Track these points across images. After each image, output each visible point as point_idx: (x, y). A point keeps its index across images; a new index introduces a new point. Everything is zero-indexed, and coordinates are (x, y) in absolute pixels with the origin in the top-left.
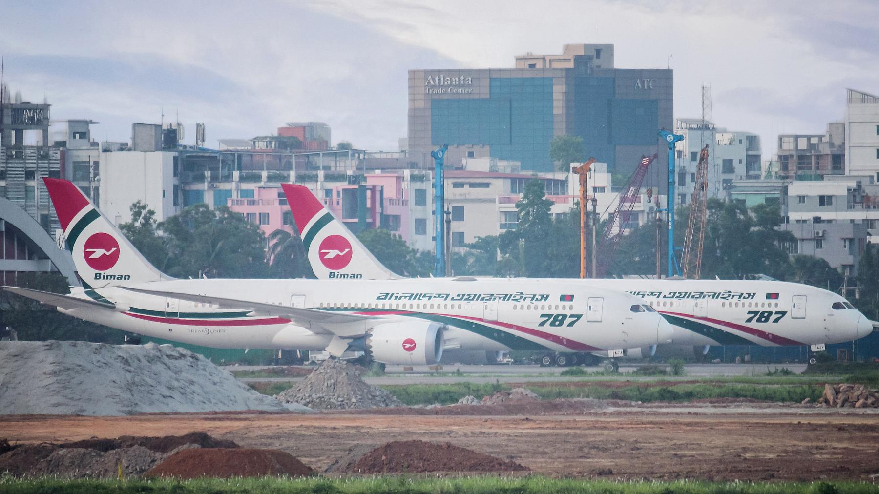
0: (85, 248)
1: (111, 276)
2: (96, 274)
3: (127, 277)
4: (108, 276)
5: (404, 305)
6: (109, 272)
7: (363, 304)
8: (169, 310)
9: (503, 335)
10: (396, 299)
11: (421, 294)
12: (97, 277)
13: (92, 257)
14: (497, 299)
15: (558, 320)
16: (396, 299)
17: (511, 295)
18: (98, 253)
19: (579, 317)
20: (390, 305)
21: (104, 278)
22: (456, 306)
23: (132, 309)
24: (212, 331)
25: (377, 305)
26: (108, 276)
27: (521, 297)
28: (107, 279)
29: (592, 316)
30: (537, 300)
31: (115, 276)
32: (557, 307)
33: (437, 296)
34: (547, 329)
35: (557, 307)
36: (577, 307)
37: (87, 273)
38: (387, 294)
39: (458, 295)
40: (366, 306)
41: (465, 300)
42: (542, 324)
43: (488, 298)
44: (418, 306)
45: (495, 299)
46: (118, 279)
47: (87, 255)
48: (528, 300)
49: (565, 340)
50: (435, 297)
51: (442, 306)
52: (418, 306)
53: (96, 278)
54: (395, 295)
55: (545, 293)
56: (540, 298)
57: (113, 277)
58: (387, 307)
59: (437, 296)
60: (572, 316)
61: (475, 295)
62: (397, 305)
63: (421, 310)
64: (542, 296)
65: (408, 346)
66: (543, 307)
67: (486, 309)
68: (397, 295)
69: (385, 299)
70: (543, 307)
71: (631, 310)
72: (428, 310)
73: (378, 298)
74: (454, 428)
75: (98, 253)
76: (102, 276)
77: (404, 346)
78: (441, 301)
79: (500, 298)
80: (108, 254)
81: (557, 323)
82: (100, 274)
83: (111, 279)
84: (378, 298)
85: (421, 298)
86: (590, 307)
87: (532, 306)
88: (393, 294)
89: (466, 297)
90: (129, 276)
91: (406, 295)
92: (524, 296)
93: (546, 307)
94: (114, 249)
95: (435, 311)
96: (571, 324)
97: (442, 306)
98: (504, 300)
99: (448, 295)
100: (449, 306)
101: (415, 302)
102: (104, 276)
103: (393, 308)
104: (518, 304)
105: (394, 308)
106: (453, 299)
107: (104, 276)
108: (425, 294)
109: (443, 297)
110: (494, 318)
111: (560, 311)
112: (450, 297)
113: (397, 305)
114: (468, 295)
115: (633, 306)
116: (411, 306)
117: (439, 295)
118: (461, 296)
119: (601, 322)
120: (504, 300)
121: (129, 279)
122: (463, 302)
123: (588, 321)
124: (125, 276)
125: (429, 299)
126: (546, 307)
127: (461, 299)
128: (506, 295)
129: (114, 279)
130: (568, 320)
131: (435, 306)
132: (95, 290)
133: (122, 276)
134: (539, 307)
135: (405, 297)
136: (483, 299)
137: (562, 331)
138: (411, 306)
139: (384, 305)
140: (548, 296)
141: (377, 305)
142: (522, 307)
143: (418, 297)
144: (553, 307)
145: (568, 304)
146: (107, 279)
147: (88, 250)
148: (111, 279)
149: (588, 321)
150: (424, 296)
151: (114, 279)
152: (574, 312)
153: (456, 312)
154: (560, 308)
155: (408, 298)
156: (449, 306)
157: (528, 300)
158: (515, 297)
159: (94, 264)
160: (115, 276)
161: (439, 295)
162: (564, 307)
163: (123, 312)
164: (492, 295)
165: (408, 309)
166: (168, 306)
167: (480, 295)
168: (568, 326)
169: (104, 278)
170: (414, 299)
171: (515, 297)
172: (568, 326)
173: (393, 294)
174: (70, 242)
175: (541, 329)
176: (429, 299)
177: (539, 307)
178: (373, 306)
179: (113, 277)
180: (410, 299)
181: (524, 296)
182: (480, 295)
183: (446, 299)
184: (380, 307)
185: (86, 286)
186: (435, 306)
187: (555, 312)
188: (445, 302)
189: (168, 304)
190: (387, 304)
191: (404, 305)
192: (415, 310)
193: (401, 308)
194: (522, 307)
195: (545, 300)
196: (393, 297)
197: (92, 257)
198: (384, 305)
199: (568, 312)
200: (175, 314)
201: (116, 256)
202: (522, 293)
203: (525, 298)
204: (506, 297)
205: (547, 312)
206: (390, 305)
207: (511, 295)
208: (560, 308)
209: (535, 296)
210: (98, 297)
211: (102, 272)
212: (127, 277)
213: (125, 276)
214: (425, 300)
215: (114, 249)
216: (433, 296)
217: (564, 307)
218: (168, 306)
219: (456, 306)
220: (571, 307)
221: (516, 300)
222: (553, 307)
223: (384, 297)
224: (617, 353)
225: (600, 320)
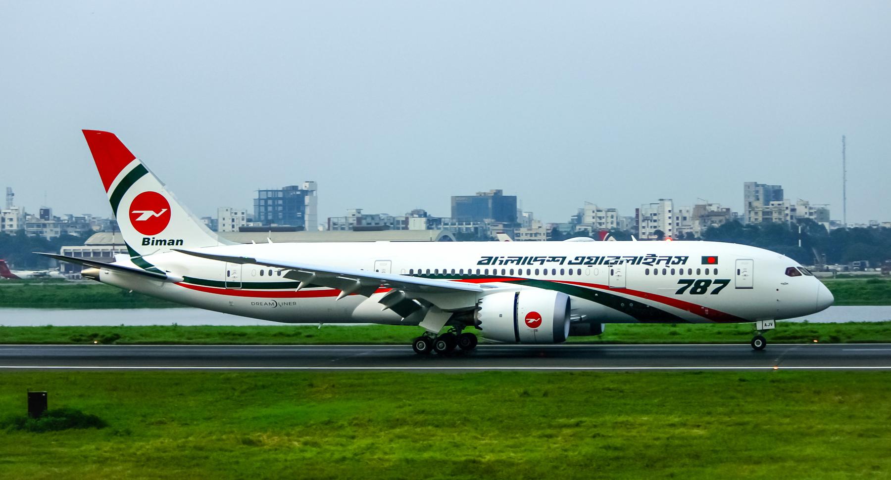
0: (132, 209)
1: (161, 241)
2: (144, 239)
3: (180, 242)
4: (157, 241)
5: (512, 272)
6: (158, 237)
7: (462, 271)
8: (230, 279)
9: (631, 305)
10: (501, 264)
11: (532, 258)
12: (145, 242)
13: (139, 219)
14: (625, 262)
15: (700, 287)
16: (501, 264)
17: (641, 258)
18: (146, 215)
19: (725, 282)
20: (495, 271)
21: (153, 244)
22: (575, 272)
23: (186, 279)
24: (281, 304)
25: (478, 271)
26: (157, 241)
27: (654, 260)
28: (157, 244)
29: (740, 281)
30: (673, 263)
31: (165, 241)
32: (699, 272)
33: (551, 259)
34: (687, 297)
35: (699, 272)
36: (724, 270)
37: (134, 238)
38: (490, 258)
39: (577, 259)
40: (466, 272)
41: (585, 264)
42: (680, 292)
43: (613, 261)
44: (529, 272)
45: (622, 262)
46: (169, 244)
47: (133, 217)
48: (663, 263)
49: (707, 311)
51: (558, 272)
52: (529, 272)
53: (143, 244)
54: (499, 259)
55: (682, 254)
56: (676, 260)
57: (163, 242)
58: (491, 273)
59: (551, 259)
60: (717, 282)
61: (597, 258)
62: (503, 271)
63: (533, 276)
64: (679, 258)
65: (532, 321)
66: (681, 272)
67: (612, 274)
68: (502, 259)
69: (488, 263)
70: (681, 272)
71: (786, 273)
72: (541, 277)
73: (480, 263)
74: (584, 419)
75: (146, 215)
76: (151, 241)
77: (527, 321)
78: (556, 265)
79: (628, 261)
80: (157, 216)
81: (699, 290)
82: (149, 239)
83: (161, 244)
84: (480, 263)
85: (532, 262)
86: (739, 271)
87: (669, 270)
88: (497, 258)
90: (182, 241)
91: (513, 259)
92: (657, 259)
93: (686, 272)
94: (164, 210)
95: (549, 277)
96: (716, 292)
97: (558, 272)
98: (633, 263)
99: (564, 258)
100: (567, 272)
101: (525, 268)
102: (153, 241)
103: (497, 275)
104: (651, 269)
105: (499, 274)
106: (570, 263)
107: (153, 241)
108: (536, 258)
109: (558, 261)
110: (621, 285)
111: (703, 276)
112: (566, 261)
113: (503, 271)
114: (589, 258)
115: (788, 269)
116: (520, 272)
117: (554, 259)
118: (580, 259)
119: (752, 288)
120: (633, 263)
121: (181, 244)
122: (583, 267)
123: (736, 288)
124: (178, 241)
125: (542, 264)
126: (686, 272)
127: (580, 263)
128: (636, 258)
129: (165, 244)
130: (712, 287)
131: (550, 272)
132: (143, 258)
133: (173, 241)
134: (677, 272)
135: (512, 262)
136: (607, 263)
137: (705, 300)
138: (520, 272)
139: (487, 271)
140: (686, 258)
141: (478, 271)
142: (656, 272)
143: (529, 261)
144: (694, 272)
145: (711, 267)
146: (157, 244)
147: (134, 212)
148: (161, 244)
149: (736, 288)
150: (536, 260)
151: (165, 244)
152: (718, 277)
153: (575, 278)
154: (703, 272)
155: (516, 262)
156: (567, 272)
157: (663, 263)
158: (646, 259)
159: (140, 227)
161: (554, 259)
162: (707, 272)
163: (177, 283)
164: (618, 258)
165: (516, 275)
166: (229, 275)
167: (603, 258)
168: (712, 293)
169: (153, 244)
170: (523, 263)
171: (646, 259)
172: (712, 293)
173: (497, 258)
174: (115, 201)
175: (679, 297)
176: (542, 264)
177: (677, 272)
178: (474, 272)
179: (163, 242)
180: (518, 264)
181: (657, 259)
182: (603, 258)
183: (562, 263)
184: (482, 273)
185: (131, 252)
186: (550, 272)
187: (695, 277)
188: (562, 267)
189: (229, 272)
190: (491, 268)
191: (512, 272)
192: (524, 276)
193: (508, 274)
194: (656, 272)
195: (684, 263)
196: (498, 262)
197: (139, 219)
198: (487, 271)
199: (712, 277)
200: (237, 284)
201: (166, 218)
202: (654, 255)
203: (659, 261)
204: (635, 260)
205: (686, 276)
206: (495, 271)
208: (703, 272)
209: (670, 258)
210: (146, 265)
211: (151, 237)
212: (180, 242)
213: (178, 241)
214: (537, 265)
215: (164, 210)
216: (547, 259)
217: (707, 272)
218: (229, 275)
219: (575, 272)
220: (716, 272)
221: (648, 264)
222: (694, 272)
223: (486, 261)
224: (768, 324)
225: (751, 286)
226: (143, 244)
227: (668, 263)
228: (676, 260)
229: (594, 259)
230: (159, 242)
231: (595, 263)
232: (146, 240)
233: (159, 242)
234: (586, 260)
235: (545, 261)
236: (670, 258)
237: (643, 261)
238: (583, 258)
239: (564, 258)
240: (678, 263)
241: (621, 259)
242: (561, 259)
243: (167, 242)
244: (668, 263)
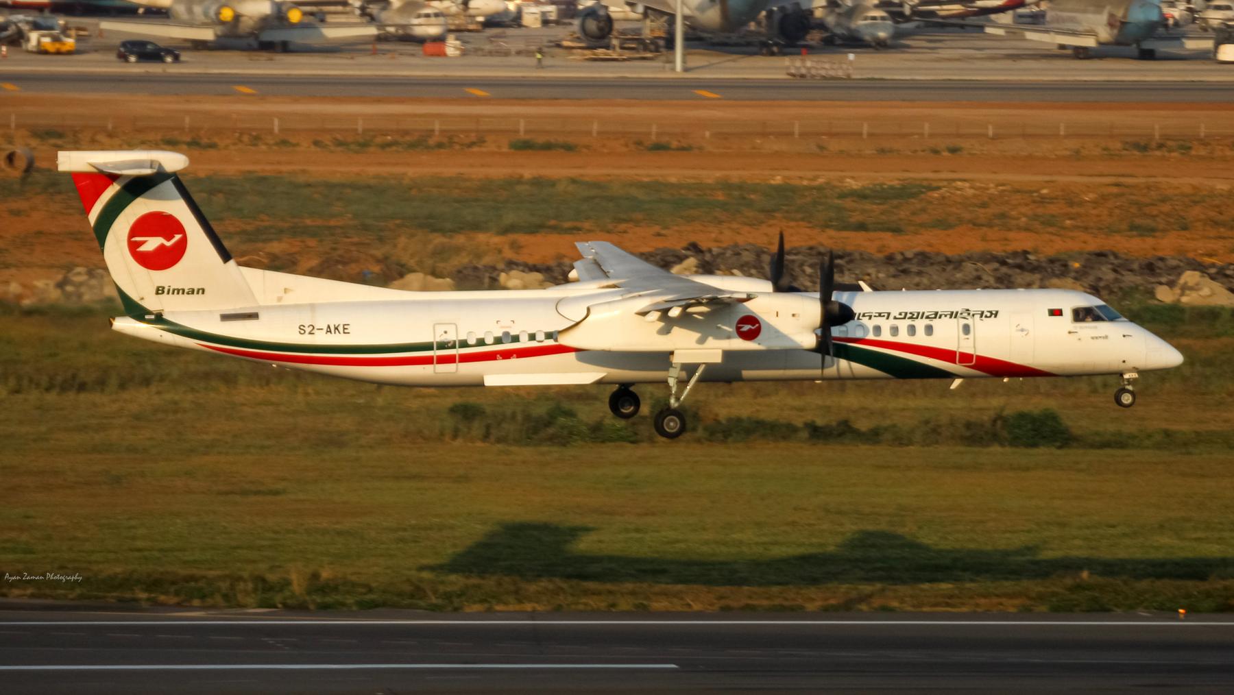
1: (178, 290)
14: (943, 316)
17: (957, 313)
21: (168, 293)
28: (173, 293)
30: (986, 317)
39: (900, 314)
41: (909, 318)
46: (188, 293)
50: (875, 316)
55: (993, 309)
56: (989, 314)
57: (181, 292)
64: (991, 312)
76: (166, 291)
79: (946, 316)
83: (178, 293)
85: (861, 318)
89: (909, 315)
106: (895, 318)
109: (884, 316)
114: (911, 313)
117: (880, 315)
118: (903, 314)
125: (870, 319)
127: (904, 318)
129: (183, 293)
136: (927, 317)
140: (997, 312)
148: (178, 293)
150: (864, 316)
160: (183, 290)
161: (880, 315)
167: (923, 313)
179: (181, 292)
182: (923, 313)
183: (888, 318)
202: (968, 310)
203: (973, 315)
207: (957, 313)
209: (983, 312)
226: (157, 293)
227: (981, 317)
228: (989, 314)
229: (916, 314)
230: (176, 291)
231: (917, 318)
232: (160, 289)
233: (176, 291)
234: (909, 315)
235: (873, 317)
236: (983, 312)
237: (959, 314)
238: (906, 314)
239: (889, 314)
240: (990, 317)
241: (940, 313)
242: (886, 315)
243: (186, 291)
244: (981, 317)
